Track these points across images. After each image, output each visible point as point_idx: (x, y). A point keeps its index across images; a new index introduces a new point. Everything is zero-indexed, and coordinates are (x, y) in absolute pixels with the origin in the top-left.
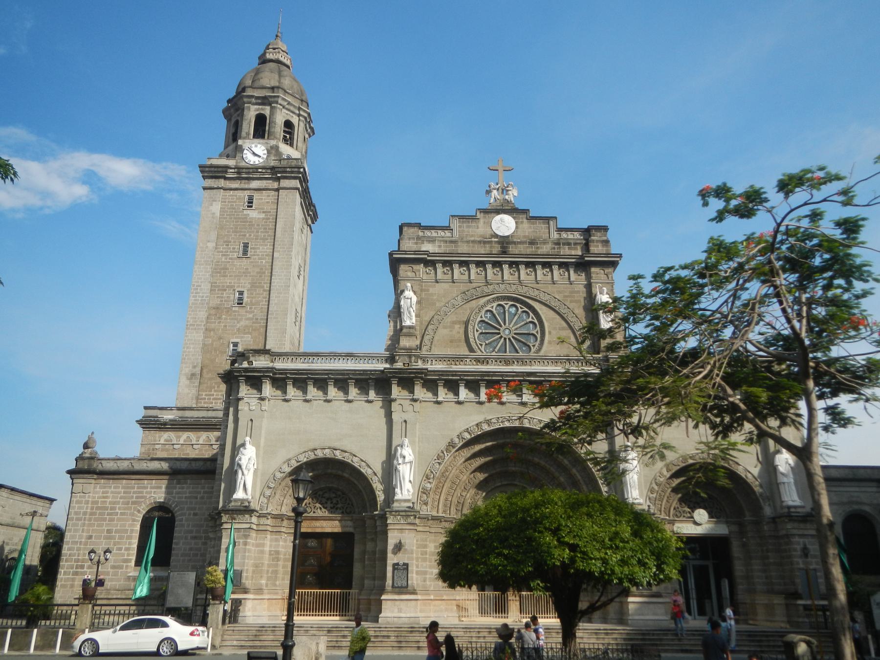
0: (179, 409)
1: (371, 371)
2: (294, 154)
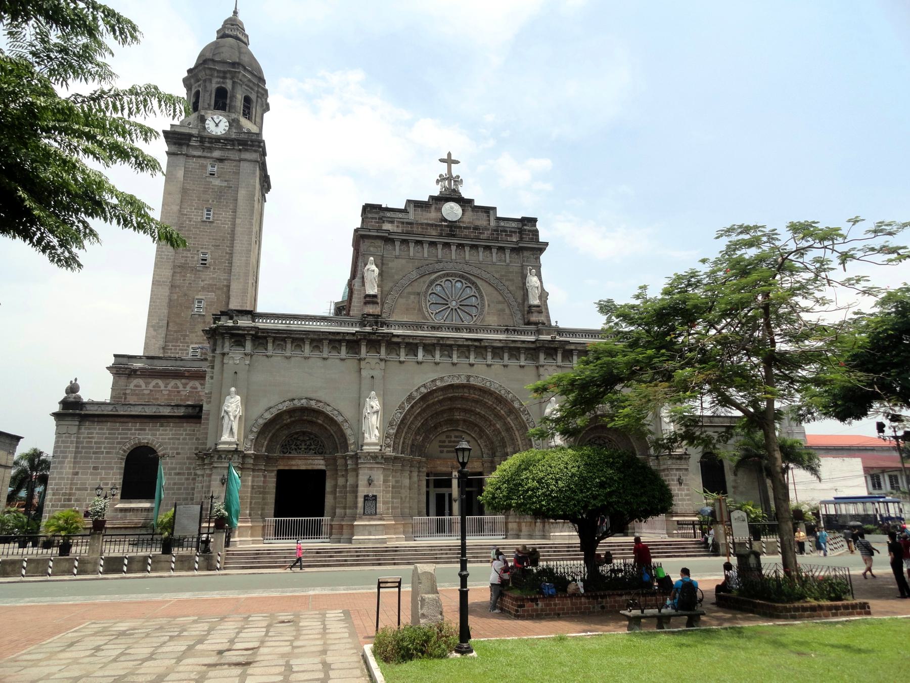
0: (148, 358)
1: (344, 333)
2: (254, 129)
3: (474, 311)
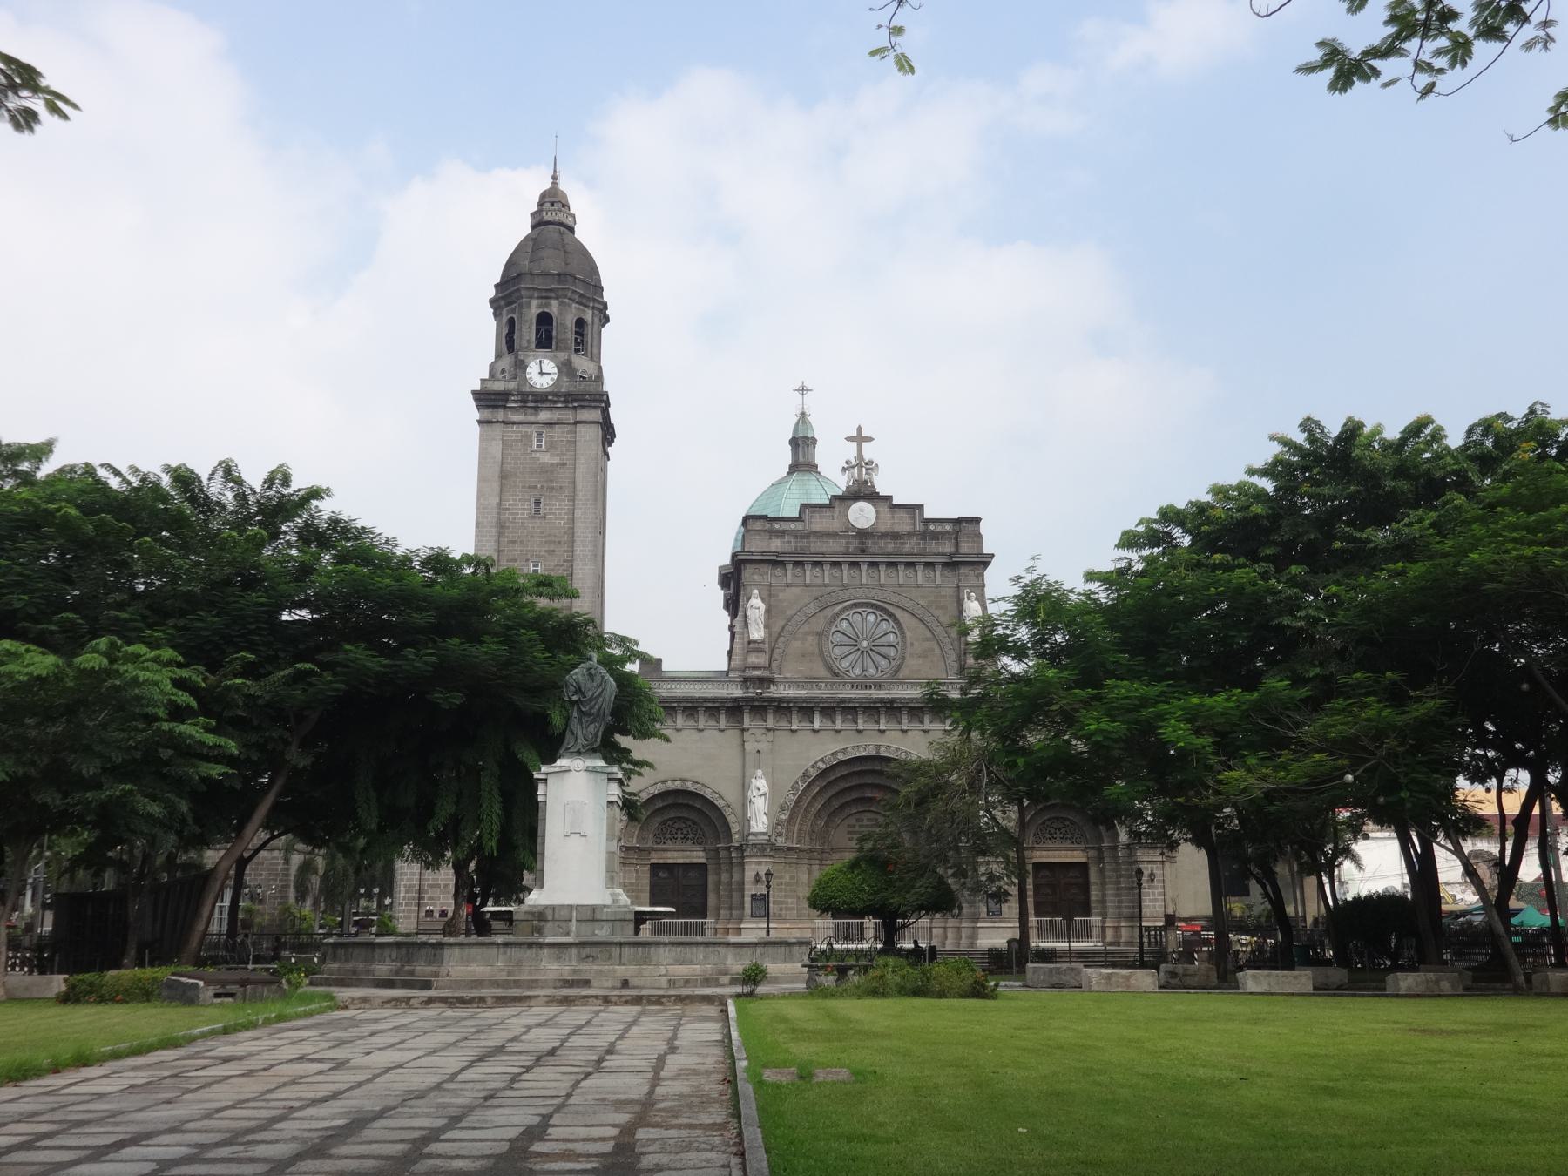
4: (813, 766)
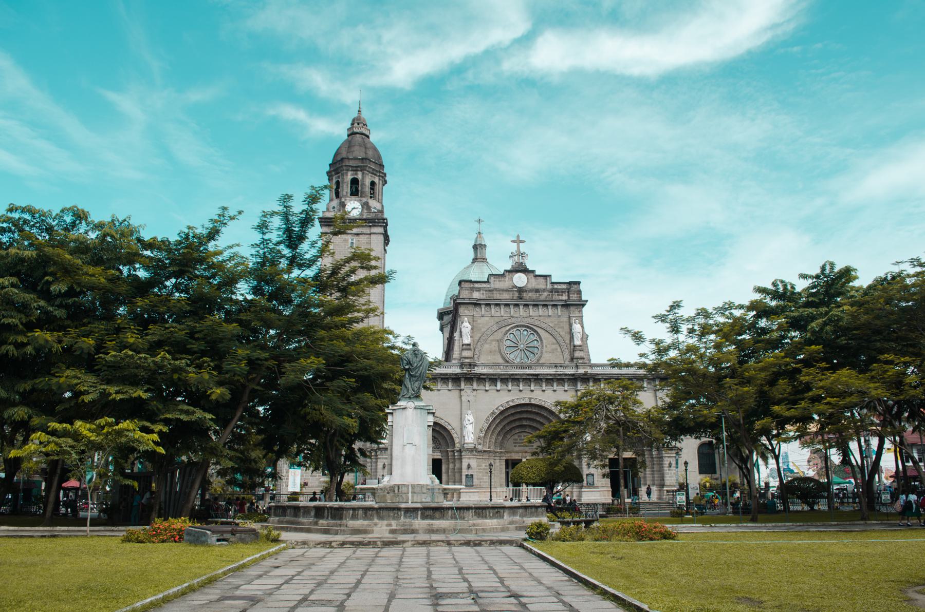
2: (379, 207)
3: (536, 351)
4: (497, 409)
